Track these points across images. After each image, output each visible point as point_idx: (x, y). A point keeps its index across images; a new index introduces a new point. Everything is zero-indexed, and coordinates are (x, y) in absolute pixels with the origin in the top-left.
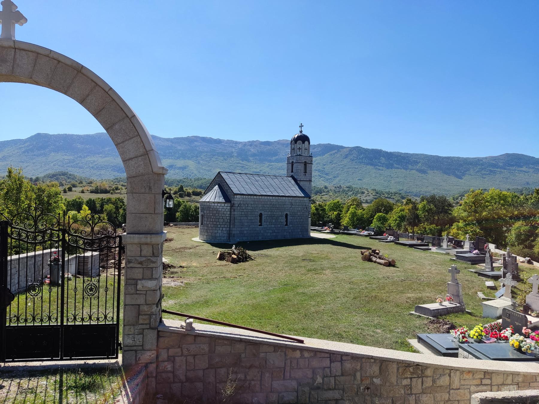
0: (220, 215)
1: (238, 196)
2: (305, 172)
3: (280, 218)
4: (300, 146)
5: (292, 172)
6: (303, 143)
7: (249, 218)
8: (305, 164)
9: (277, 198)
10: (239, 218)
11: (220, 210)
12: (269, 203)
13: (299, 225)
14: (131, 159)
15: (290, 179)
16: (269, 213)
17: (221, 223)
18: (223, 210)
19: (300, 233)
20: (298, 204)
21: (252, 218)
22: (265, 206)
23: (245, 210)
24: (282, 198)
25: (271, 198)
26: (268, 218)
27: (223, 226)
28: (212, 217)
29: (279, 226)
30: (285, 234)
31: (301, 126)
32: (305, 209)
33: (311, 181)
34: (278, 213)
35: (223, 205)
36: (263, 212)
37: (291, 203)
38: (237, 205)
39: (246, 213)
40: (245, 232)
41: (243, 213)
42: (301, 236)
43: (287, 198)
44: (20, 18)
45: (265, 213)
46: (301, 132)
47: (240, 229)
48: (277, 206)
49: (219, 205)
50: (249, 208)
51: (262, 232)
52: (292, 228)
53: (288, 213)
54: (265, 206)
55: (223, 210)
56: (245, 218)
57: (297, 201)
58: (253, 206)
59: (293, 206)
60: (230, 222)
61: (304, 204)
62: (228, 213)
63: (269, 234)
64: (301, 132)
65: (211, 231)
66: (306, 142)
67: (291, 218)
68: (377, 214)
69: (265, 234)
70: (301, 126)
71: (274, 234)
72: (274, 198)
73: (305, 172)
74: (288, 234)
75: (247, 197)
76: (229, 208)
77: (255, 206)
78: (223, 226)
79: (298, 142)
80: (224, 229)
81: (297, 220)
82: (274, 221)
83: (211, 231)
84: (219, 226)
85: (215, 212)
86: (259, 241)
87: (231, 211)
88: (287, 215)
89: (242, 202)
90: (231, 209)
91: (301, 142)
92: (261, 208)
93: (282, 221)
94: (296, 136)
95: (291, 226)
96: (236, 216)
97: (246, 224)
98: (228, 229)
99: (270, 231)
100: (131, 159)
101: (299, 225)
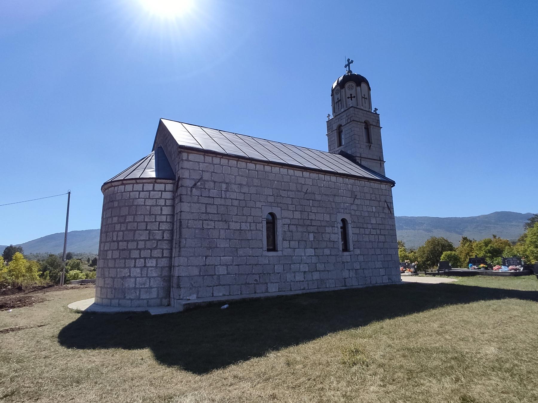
0: (139, 219)
1: (192, 157)
2: (369, 141)
3: (328, 230)
4: (353, 92)
7: (233, 226)
10: (199, 224)
11: (141, 202)
12: (293, 187)
13: (378, 252)
16: (297, 215)
17: (141, 245)
18: (149, 202)
19: (382, 272)
20: (368, 196)
21: (244, 226)
22: (283, 193)
23: (218, 201)
24: (327, 177)
25: (298, 173)
26: (293, 228)
27: (146, 253)
28: (118, 227)
29: (327, 252)
30: (346, 274)
31: (350, 62)
32: (387, 211)
34: (319, 217)
35: (149, 187)
36: (276, 211)
37: (352, 192)
38: (190, 183)
39: (222, 210)
40: (222, 270)
41: (212, 209)
42: (386, 281)
43: (340, 179)
45: (285, 214)
47: (200, 261)
48: (318, 197)
49: (139, 187)
50: (234, 196)
51: (278, 268)
52: (361, 258)
54: (283, 193)
55: (149, 202)
56: (221, 225)
57: (366, 190)
58: (245, 190)
59: (357, 202)
60: (171, 241)
62: (167, 211)
63: (299, 277)
65: (113, 273)
66: (363, 85)
67: (357, 231)
68: (444, 253)
69: (289, 277)
70: (350, 62)
71: (316, 276)
73: (369, 141)
74: (352, 274)
75: (224, 161)
76: (168, 195)
77: (253, 190)
78: (146, 253)
79: (347, 85)
80: (151, 263)
81: (372, 238)
82: (311, 236)
83: (113, 273)
85: (124, 211)
86: (267, 299)
87: (173, 206)
88: (344, 221)
89: (206, 176)
90: (173, 199)
91: (354, 84)
92: (271, 199)
93: (334, 237)
95: (358, 252)
96: (184, 216)
97: (223, 244)
98: (164, 262)
99: (304, 268)
101: (378, 252)
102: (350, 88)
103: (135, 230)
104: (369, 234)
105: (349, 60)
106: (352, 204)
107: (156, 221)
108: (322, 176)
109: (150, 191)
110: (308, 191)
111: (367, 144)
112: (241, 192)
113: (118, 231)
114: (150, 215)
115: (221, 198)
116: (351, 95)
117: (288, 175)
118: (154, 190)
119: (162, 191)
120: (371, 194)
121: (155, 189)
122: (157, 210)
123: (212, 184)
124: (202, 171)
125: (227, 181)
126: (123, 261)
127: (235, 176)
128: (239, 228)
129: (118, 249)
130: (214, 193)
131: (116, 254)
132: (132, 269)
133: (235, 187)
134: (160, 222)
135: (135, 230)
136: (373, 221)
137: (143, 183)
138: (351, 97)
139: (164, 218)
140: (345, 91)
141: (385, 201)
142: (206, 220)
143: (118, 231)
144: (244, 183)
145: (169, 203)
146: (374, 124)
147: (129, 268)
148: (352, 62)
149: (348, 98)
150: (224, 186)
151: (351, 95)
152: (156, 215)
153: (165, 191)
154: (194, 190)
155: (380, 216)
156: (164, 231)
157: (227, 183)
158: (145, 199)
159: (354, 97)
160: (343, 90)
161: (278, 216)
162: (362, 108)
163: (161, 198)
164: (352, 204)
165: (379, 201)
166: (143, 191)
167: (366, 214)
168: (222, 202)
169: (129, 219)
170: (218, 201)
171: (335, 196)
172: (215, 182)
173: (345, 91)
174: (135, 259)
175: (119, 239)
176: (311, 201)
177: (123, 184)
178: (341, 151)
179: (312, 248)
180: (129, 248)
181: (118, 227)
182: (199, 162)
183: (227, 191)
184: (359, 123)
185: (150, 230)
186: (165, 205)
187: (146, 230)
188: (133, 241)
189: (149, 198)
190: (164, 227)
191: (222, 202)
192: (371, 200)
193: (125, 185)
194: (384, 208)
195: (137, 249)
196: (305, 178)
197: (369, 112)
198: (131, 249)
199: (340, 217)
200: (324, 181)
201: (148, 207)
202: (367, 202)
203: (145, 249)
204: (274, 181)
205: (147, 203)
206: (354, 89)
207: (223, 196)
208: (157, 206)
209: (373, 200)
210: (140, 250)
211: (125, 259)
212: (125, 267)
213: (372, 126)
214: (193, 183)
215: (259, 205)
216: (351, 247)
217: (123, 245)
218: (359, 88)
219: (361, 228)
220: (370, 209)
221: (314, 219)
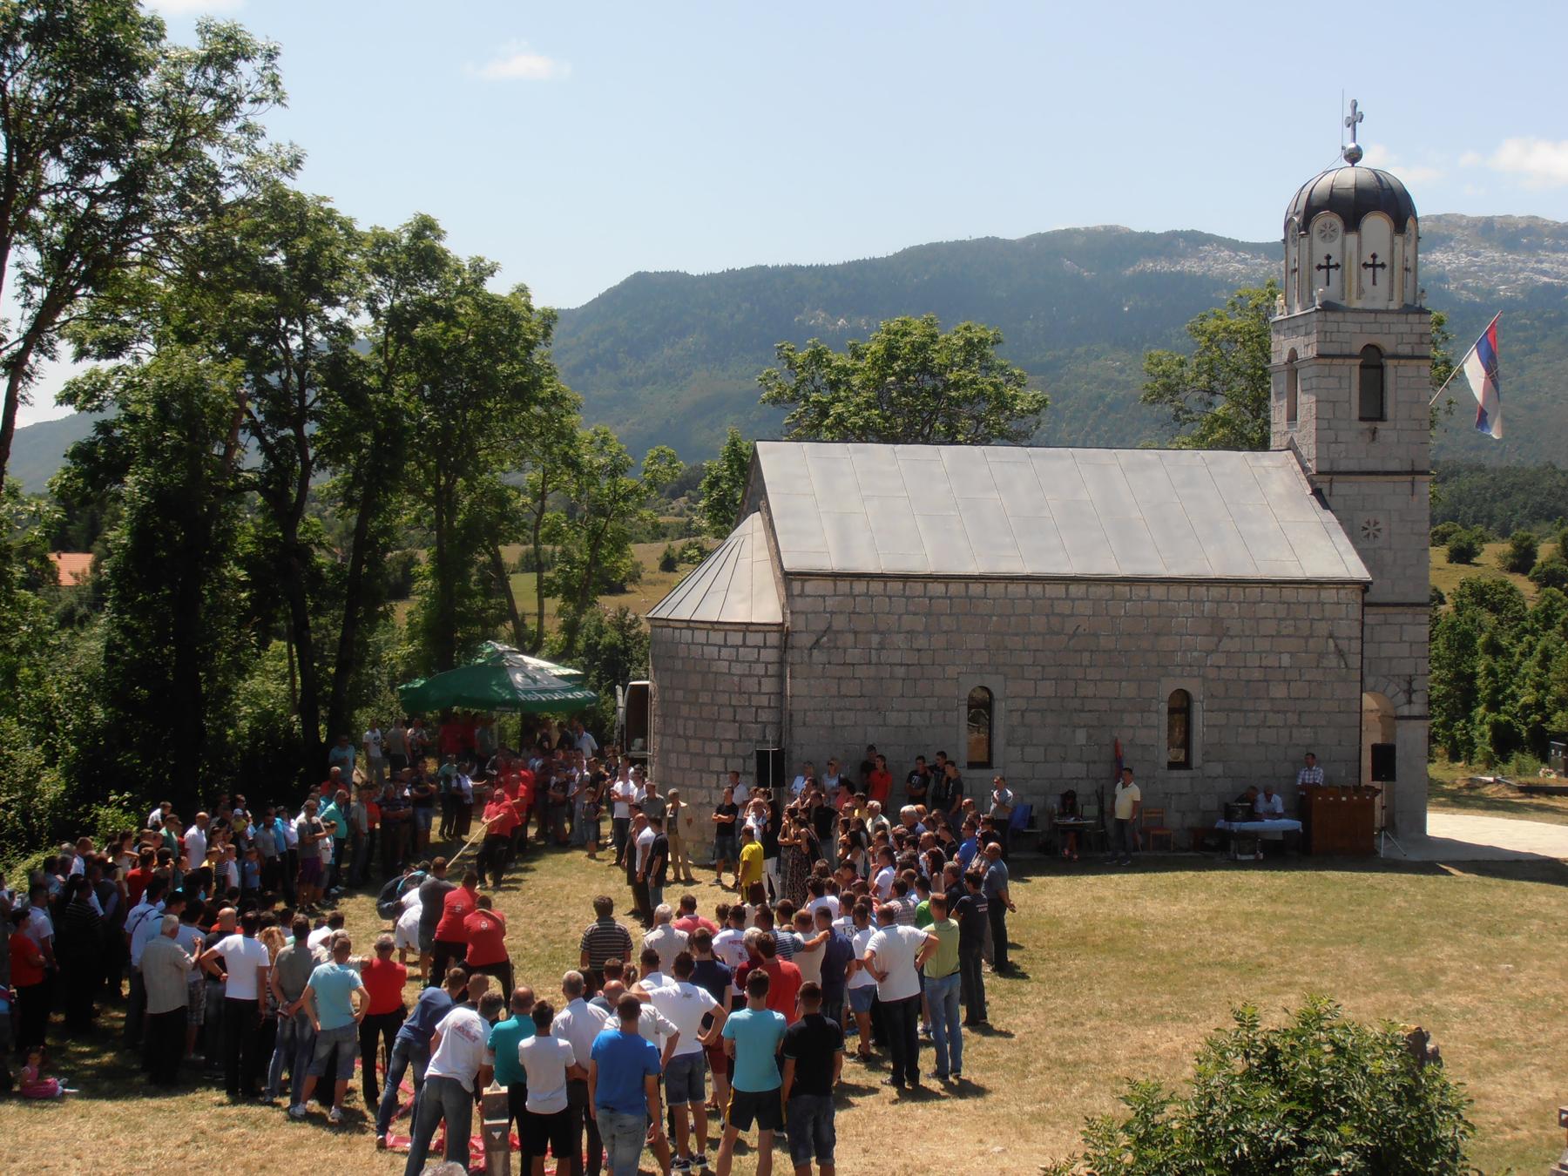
4: (1333, 248)
7: (894, 718)
8: (1373, 363)
16: (1047, 688)
20: (1269, 627)
23: (861, 672)
28: (685, 710)
31: (1354, 121)
32: (1332, 661)
36: (995, 684)
37: (1215, 619)
46: (1354, 156)
49: (717, 638)
50: (896, 657)
53: (1194, 687)
55: (738, 669)
58: (922, 642)
59: (1227, 644)
61: (1322, 628)
62: (769, 685)
70: (1354, 121)
76: (770, 655)
79: (1317, 224)
84: (717, 764)
89: (839, 623)
90: (782, 663)
91: (1338, 223)
102: (1327, 236)
103: (716, 721)
104: (1257, 727)
106: (1208, 653)
107: (750, 706)
109: (737, 647)
110: (1081, 630)
112: (911, 649)
113: (687, 719)
114: (740, 693)
115: (870, 663)
116: (1328, 258)
117: (1027, 597)
118: (744, 645)
119: (759, 648)
120: (1281, 619)
121: (749, 642)
122: (751, 685)
123: (851, 637)
124: (832, 613)
125: (882, 627)
126: (697, 775)
127: (900, 616)
128: (905, 723)
129: (687, 752)
130: (854, 655)
131: (685, 762)
132: (715, 792)
133: (899, 640)
134: (757, 708)
135: (716, 721)
136: (1279, 691)
137: (726, 631)
139: (764, 701)
140: (1311, 244)
142: (839, 710)
143: (687, 719)
144: (921, 628)
145: (772, 669)
146: (1405, 349)
147: (709, 788)
149: (1319, 267)
150: (875, 639)
151: (1328, 258)
152: (750, 694)
153: (765, 646)
154: (815, 652)
155: (1307, 677)
156: (765, 724)
157: (882, 633)
158: (730, 662)
160: (1305, 241)
161: (996, 695)
162: (1357, 304)
163: (757, 661)
164: (1208, 653)
165: (1307, 638)
166: (726, 646)
167: (1257, 675)
168: (872, 671)
169: (704, 698)
170: (861, 672)
171: (1157, 635)
172: (855, 633)
173: (1311, 244)
174: (718, 773)
175: (690, 733)
176: (1086, 655)
177: (688, 628)
179: (1080, 761)
180: (708, 750)
181: (685, 710)
182: (823, 597)
183: (881, 647)
184: (1335, 361)
185: (741, 723)
186: (766, 675)
187: (734, 721)
188: (713, 739)
189: (737, 661)
190: (764, 716)
191: (872, 671)
192: (1279, 635)
193: (693, 629)
194: (1322, 655)
195: (720, 755)
196: (1073, 600)
197: (1387, 312)
198: (710, 756)
199: (1168, 687)
200: (1130, 600)
201: (736, 679)
202: (1264, 644)
203: (734, 756)
204: (990, 616)
205: (733, 671)
206: (1338, 241)
207: (874, 659)
208: (750, 675)
209: (1289, 636)
210: (726, 757)
211: (701, 771)
212: (701, 787)
213: (1390, 363)
214: (812, 639)
215: (951, 671)
216: (1196, 759)
217: (695, 745)
218: (1352, 238)
219: (1233, 711)
220: (1270, 661)
221: (1090, 694)
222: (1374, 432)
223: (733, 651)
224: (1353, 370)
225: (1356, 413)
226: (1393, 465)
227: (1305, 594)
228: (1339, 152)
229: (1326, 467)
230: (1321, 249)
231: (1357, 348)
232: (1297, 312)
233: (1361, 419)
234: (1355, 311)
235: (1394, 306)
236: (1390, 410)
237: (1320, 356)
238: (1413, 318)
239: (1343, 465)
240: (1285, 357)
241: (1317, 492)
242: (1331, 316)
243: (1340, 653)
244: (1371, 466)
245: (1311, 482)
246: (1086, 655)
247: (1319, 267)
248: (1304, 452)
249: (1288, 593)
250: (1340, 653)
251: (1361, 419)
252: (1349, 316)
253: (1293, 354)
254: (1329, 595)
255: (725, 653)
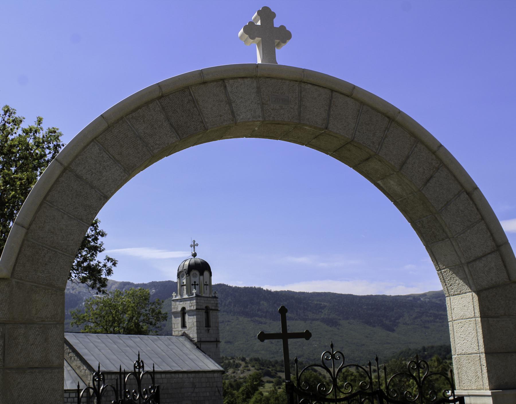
2: (208, 325)
4: (197, 280)
5: (184, 326)
6: (202, 274)
8: (207, 310)
9: (168, 376)
14: (479, 258)
15: (182, 339)
24: (177, 375)
31: (194, 245)
32: (217, 394)
33: (217, 341)
43: (186, 375)
44: (284, 35)
46: (195, 255)
64: (195, 255)
66: (206, 273)
70: (194, 245)
72: (163, 376)
73: (208, 325)
91: (198, 273)
94: (187, 263)
100: (479, 258)
102: (195, 276)
105: (194, 241)
108: (173, 375)
111: (206, 328)
116: (195, 282)
138: (195, 285)
141: (217, 387)
146: (213, 308)
148: (197, 245)
149: (192, 285)
151: (195, 282)
159: (198, 285)
162: (204, 295)
176: (166, 395)
178: (184, 332)
197: (209, 297)
206: (198, 278)
213: (211, 311)
218: (202, 277)
222: (209, 330)
223: (72, 399)
224: (203, 313)
225: (204, 326)
226: (213, 339)
227: (211, 375)
228: (191, 254)
229: (199, 340)
230: (193, 280)
231: (204, 307)
232: (186, 296)
233: (206, 327)
234: (204, 297)
235: (211, 296)
236: (212, 324)
237: (197, 309)
238: (215, 299)
239: (203, 339)
240: (179, 309)
241: (198, 347)
242: (199, 298)
243: (219, 391)
244: (208, 339)
245: (195, 344)
246: (166, 395)
247: (192, 285)
248: (191, 336)
249: (208, 375)
250: (219, 391)
251: (206, 327)
252: (202, 298)
253: (183, 309)
254: (216, 375)
255: (69, 400)
